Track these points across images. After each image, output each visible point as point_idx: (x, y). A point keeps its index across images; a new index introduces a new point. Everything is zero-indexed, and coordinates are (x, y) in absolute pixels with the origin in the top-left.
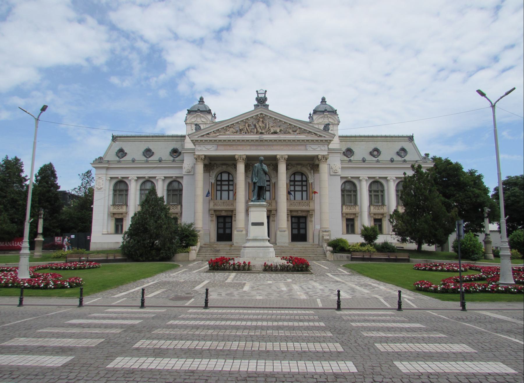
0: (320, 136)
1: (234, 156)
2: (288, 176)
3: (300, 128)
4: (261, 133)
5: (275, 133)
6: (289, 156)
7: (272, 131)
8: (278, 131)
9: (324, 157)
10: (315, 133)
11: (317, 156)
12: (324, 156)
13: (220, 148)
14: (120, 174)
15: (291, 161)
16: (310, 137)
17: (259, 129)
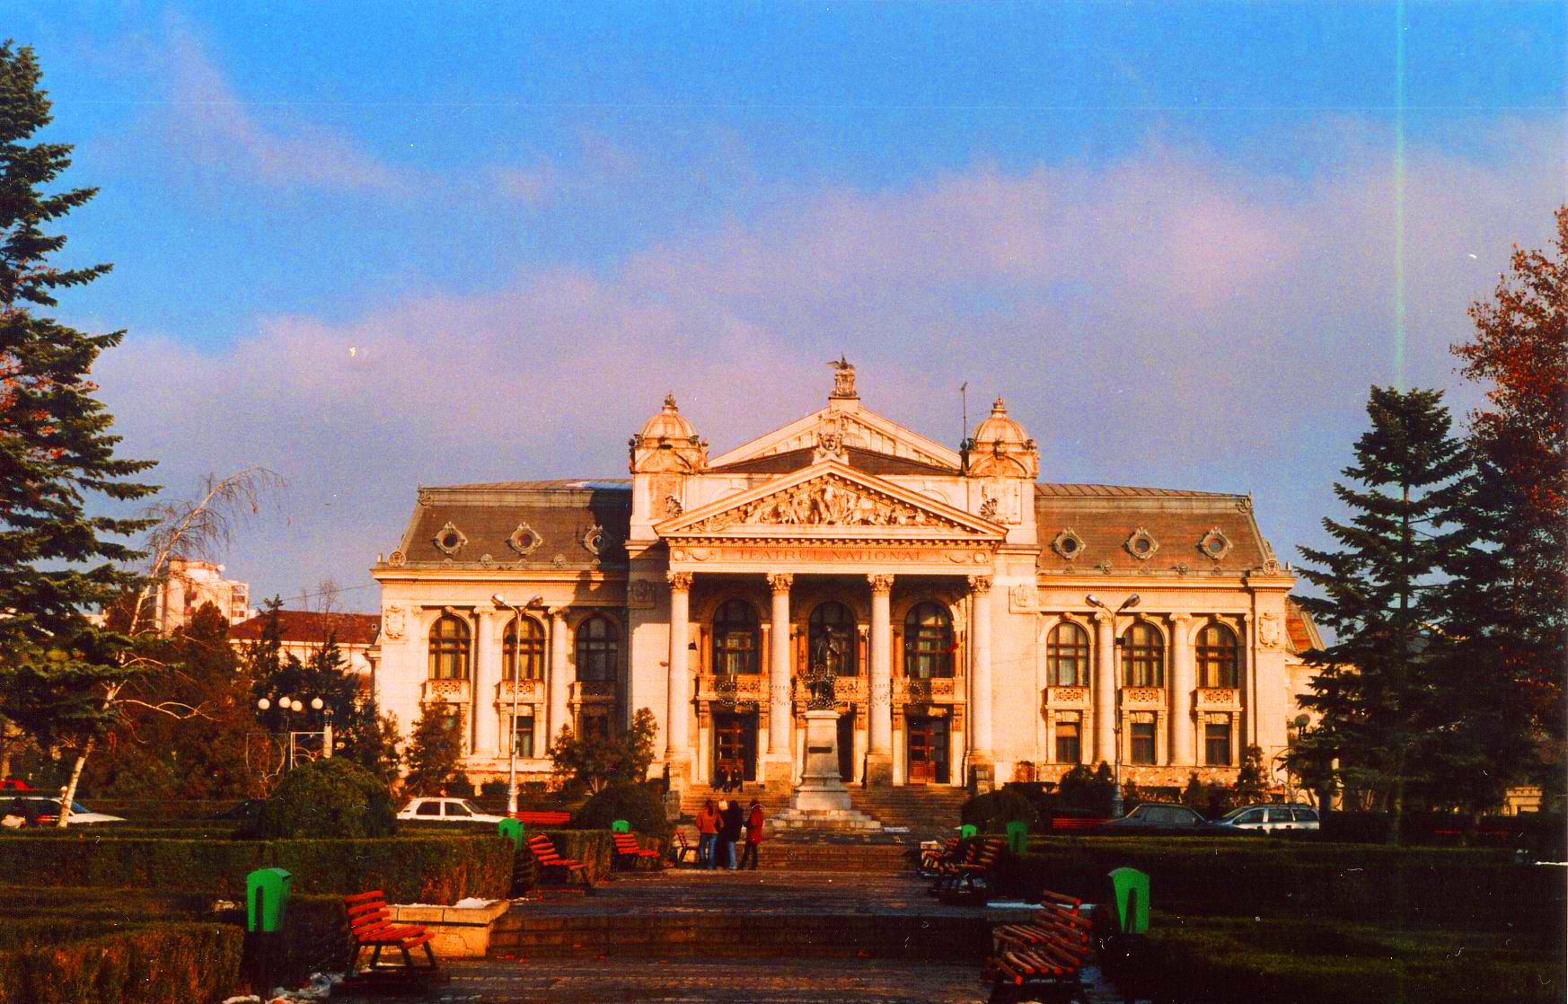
0: (974, 531)
1: (764, 575)
2: (901, 616)
3: (923, 510)
4: (831, 523)
5: (865, 522)
6: (896, 576)
7: (858, 516)
8: (871, 519)
9: (981, 581)
10: (960, 524)
11: (965, 578)
12: (979, 579)
13: (728, 557)
14: (450, 597)
15: (903, 588)
16: (945, 533)
17: (825, 515)
